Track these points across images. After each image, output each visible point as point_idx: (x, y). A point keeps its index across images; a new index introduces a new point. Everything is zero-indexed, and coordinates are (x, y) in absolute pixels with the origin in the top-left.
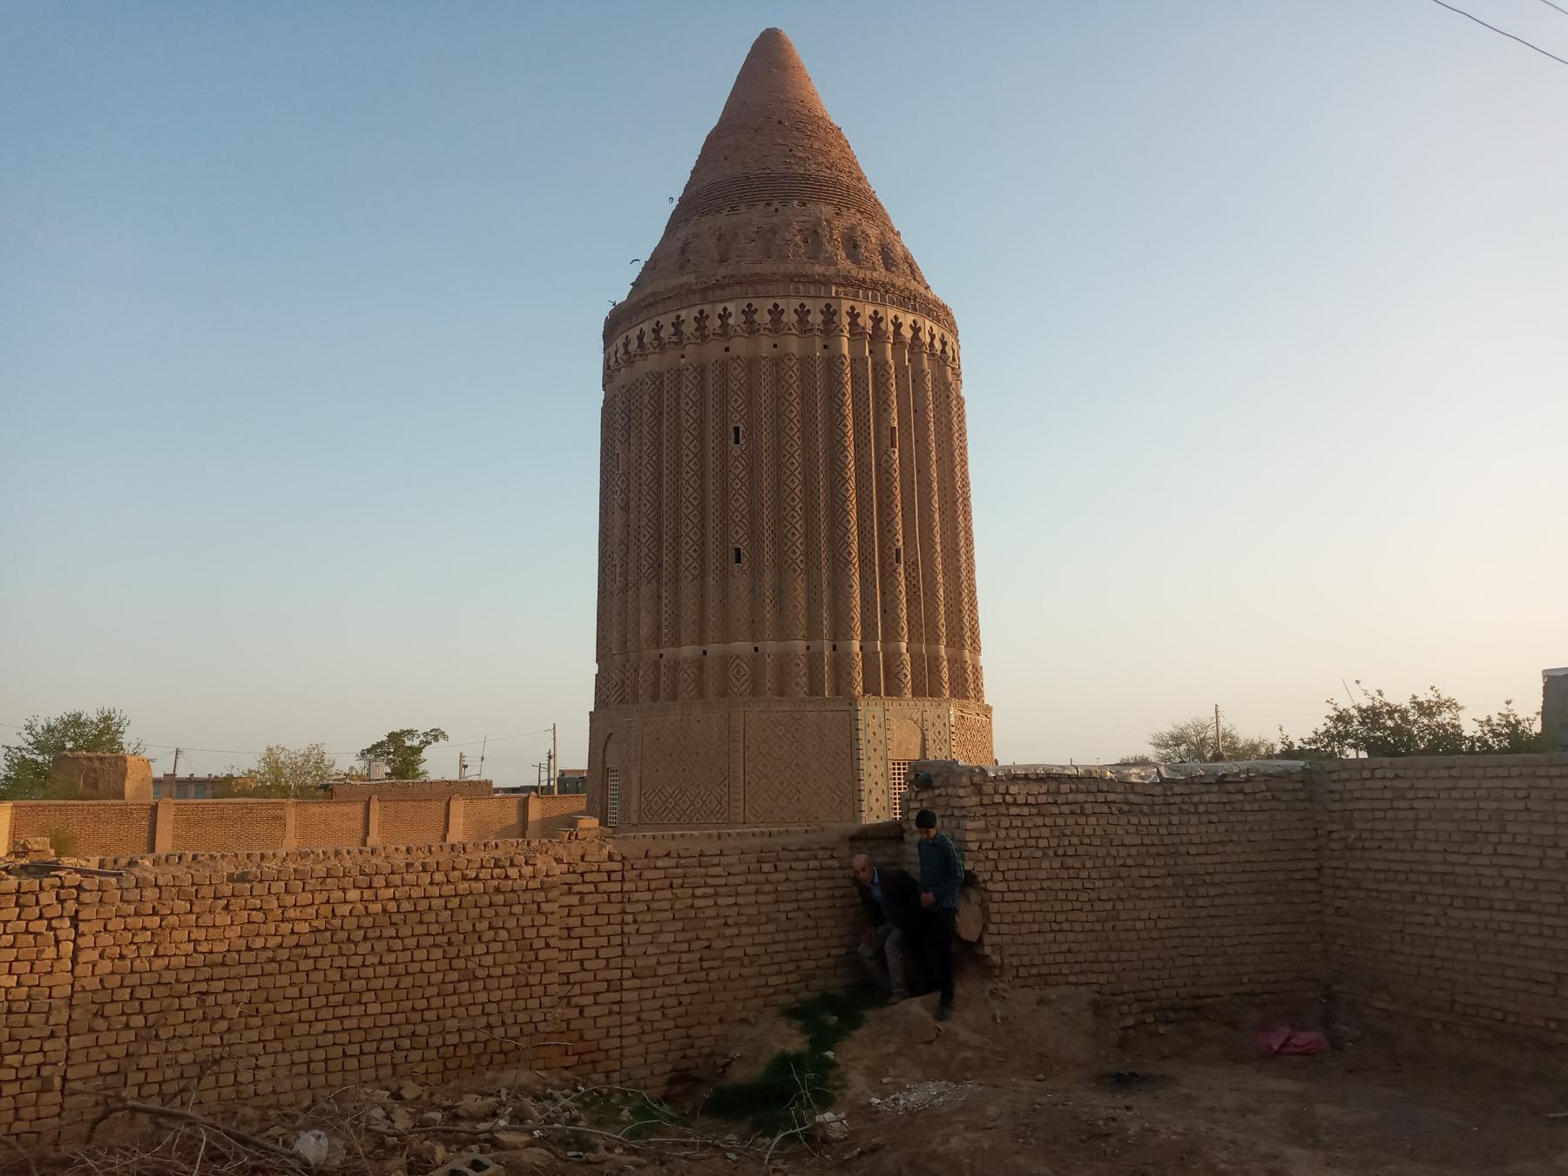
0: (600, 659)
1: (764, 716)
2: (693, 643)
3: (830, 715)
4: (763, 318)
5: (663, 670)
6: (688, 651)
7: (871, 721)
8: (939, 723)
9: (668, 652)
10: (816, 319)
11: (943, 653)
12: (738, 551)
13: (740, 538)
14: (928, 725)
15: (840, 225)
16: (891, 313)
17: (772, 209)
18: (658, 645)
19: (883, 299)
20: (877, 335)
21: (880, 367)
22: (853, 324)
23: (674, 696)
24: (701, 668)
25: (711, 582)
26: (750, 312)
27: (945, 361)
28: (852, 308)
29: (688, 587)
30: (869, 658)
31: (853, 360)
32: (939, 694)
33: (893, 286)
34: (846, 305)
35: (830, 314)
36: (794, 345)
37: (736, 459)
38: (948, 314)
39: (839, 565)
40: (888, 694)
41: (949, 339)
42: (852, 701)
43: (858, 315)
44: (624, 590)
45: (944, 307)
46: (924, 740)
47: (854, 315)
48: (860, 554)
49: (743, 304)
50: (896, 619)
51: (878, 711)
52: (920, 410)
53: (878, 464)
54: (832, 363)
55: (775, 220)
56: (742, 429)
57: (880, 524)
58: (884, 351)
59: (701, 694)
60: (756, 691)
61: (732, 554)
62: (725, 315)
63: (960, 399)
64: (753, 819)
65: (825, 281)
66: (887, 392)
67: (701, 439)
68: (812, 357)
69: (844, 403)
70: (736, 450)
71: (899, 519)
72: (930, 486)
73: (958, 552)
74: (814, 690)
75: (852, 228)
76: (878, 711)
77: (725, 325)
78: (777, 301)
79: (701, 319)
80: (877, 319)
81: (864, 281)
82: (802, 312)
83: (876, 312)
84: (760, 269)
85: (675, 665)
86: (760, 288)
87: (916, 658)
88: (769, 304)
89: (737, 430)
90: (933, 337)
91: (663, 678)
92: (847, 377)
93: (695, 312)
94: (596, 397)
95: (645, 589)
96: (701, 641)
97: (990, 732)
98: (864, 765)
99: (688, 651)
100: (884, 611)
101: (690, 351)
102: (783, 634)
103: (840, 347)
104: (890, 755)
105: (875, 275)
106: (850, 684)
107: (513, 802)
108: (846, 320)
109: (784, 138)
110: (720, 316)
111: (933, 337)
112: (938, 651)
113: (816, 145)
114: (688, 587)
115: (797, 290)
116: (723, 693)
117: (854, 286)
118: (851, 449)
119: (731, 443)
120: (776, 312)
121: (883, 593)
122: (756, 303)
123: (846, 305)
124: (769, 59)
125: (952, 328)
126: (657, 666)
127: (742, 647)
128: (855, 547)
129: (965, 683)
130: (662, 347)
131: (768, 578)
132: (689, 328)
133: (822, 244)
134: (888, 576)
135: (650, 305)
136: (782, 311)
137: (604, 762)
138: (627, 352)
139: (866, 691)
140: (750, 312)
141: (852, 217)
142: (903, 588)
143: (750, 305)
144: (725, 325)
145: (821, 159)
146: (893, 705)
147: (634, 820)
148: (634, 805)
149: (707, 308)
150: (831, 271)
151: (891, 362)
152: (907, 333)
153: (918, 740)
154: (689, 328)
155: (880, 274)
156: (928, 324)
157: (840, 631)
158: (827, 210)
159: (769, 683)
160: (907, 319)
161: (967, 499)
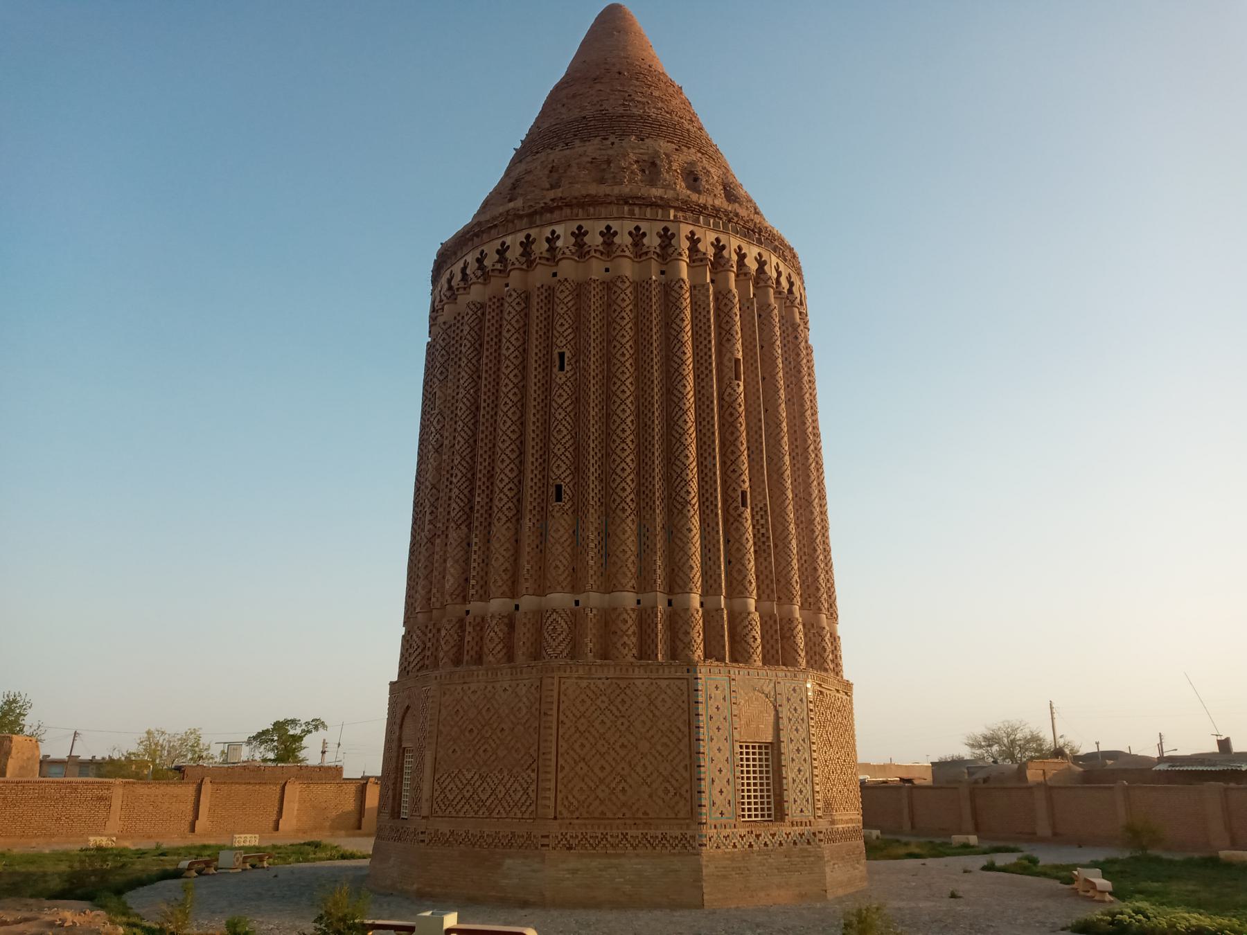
0: (406, 622)
1: (584, 683)
2: (503, 595)
3: (664, 684)
4: (594, 239)
5: (469, 629)
6: (497, 605)
7: (714, 692)
8: (795, 698)
9: (475, 606)
10: (652, 241)
11: (797, 614)
12: (559, 488)
13: (561, 472)
14: (782, 700)
15: (679, 161)
16: (733, 242)
17: (609, 142)
18: (465, 600)
20: (719, 263)
21: (722, 297)
22: (694, 249)
23: (479, 660)
24: (511, 626)
25: (527, 523)
26: (580, 234)
27: (791, 300)
28: (692, 233)
29: (501, 530)
30: (711, 616)
31: (693, 287)
32: (794, 663)
33: (737, 215)
34: (685, 229)
35: (667, 237)
36: (627, 268)
37: (561, 387)
38: (794, 256)
39: (675, 506)
40: (734, 660)
41: (794, 278)
42: (691, 667)
43: (699, 240)
44: (431, 541)
45: (791, 250)
46: (777, 718)
47: (694, 241)
48: (701, 496)
49: (573, 226)
50: (742, 572)
51: (722, 679)
52: (767, 346)
53: (721, 398)
54: (670, 289)
55: (610, 152)
56: (567, 354)
57: (723, 463)
58: (727, 280)
59: (510, 658)
60: (574, 652)
61: (552, 490)
62: (552, 239)
63: (808, 347)
64: (565, 813)
65: (663, 205)
66: (730, 323)
67: (523, 368)
68: (648, 281)
69: (682, 330)
70: (560, 377)
71: (744, 457)
72: (779, 425)
73: (810, 503)
74: (645, 652)
75: (692, 164)
76: (722, 679)
77: (552, 249)
78: (611, 223)
79: (527, 244)
80: (719, 247)
81: (705, 207)
82: (638, 235)
83: (718, 240)
84: (593, 189)
85: (481, 623)
86: (591, 210)
87: (767, 619)
88: (601, 226)
89: (562, 355)
90: (779, 274)
91: (468, 638)
92: (686, 302)
93: (521, 237)
94: (421, 337)
95: (453, 535)
96: (513, 593)
97: (851, 712)
98: (704, 747)
99: (497, 605)
100: (728, 562)
101: (515, 278)
102: (609, 585)
103: (679, 271)
104: (737, 736)
105: (717, 202)
106: (688, 645)
107: (352, 788)
108: (685, 244)
109: (621, 85)
110: (548, 240)
111: (779, 274)
112: (791, 612)
113: (656, 93)
114: (501, 530)
115: (632, 213)
116: (536, 654)
117: (697, 212)
118: (690, 378)
119: (556, 370)
120: (608, 234)
121: (727, 541)
122: (587, 225)
123: (685, 229)
124: (610, 28)
125: (799, 273)
126: (461, 623)
127: (560, 599)
128: (694, 485)
129: (823, 654)
130: (485, 275)
131: (593, 519)
132: (514, 253)
133: (659, 173)
134: (733, 521)
135: (477, 235)
136: (616, 233)
137: (400, 740)
138: (450, 288)
139: (707, 656)
140: (580, 234)
141: (691, 155)
142: (750, 535)
143: (580, 228)
144: (552, 249)
145: (660, 105)
146: (739, 673)
147: (425, 812)
148: (426, 793)
149: (533, 232)
150: (670, 194)
151: (735, 291)
152: (753, 266)
153: (771, 719)
154: (514, 253)
155: (720, 202)
156: (774, 260)
157: (676, 583)
158: (664, 146)
159: (590, 643)
160: (752, 251)
161: (817, 450)
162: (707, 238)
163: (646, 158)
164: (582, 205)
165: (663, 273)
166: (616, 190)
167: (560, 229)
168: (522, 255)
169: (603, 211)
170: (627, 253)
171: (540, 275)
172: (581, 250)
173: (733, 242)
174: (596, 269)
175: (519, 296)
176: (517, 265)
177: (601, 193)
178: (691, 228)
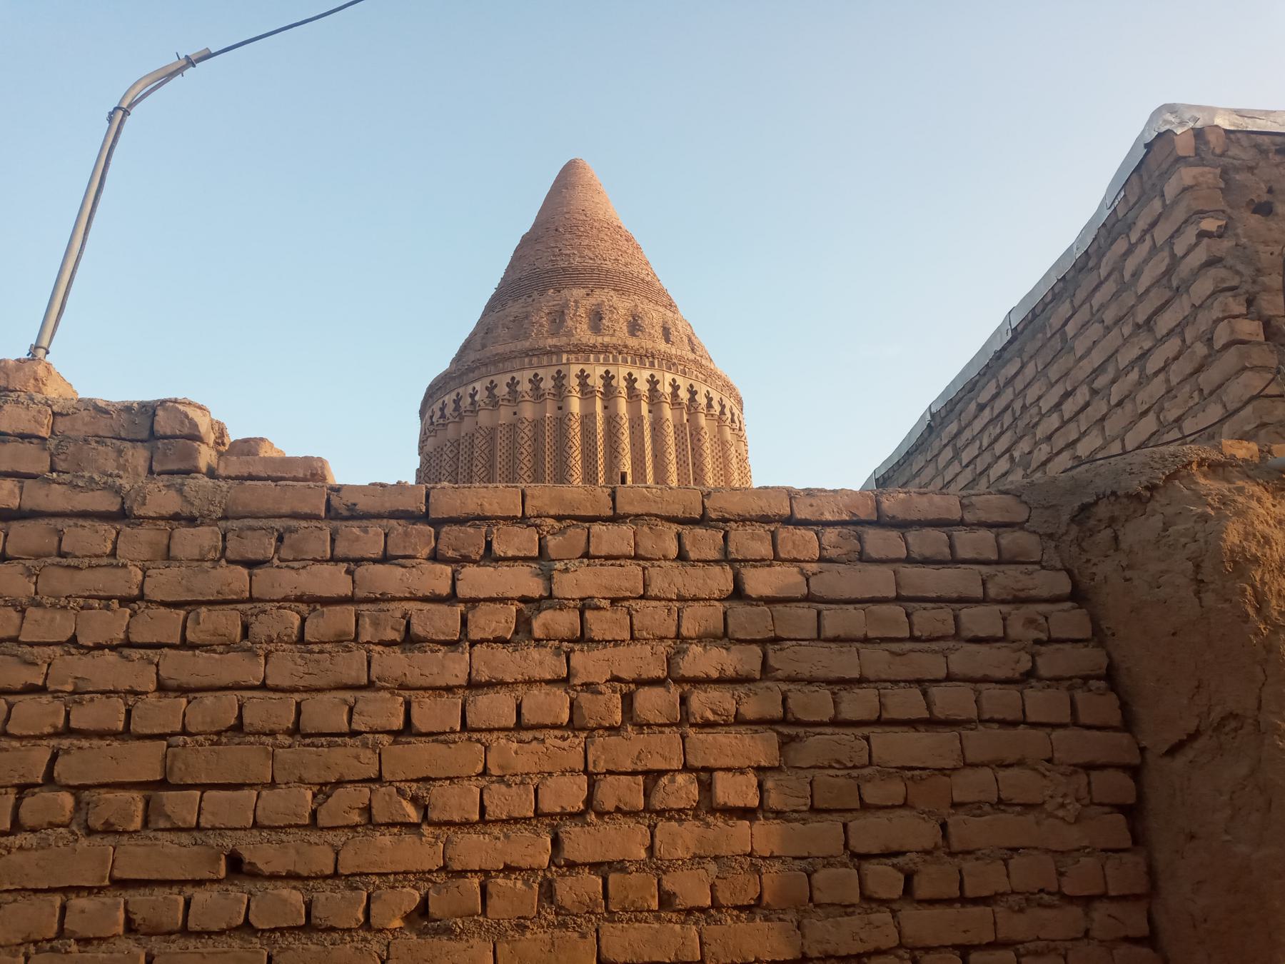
4: (502, 390)
10: (548, 384)
19: (615, 358)
21: (612, 421)
26: (491, 388)
33: (626, 346)
34: (575, 369)
35: (560, 378)
47: (583, 377)
49: (486, 382)
54: (562, 421)
55: (529, 309)
77: (473, 403)
82: (535, 381)
88: (507, 378)
93: (453, 395)
108: (574, 382)
117: (583, 351)
120: (513, 384)
122: (496, 379)
133: (564, 321)
141: (605, 296)
144: (473, 403)
149: (461, 390)
152: (642, 387)
158: (578, 293)
160: (642, 376)
162: (596, 373)
163: (557, 308)
164: (495, 363)
165: (560, 408)
166: (527, 344)
167: (478, 386)
168: (455, 410)
169: (508, 365)
170: (527, 398)
171: (467, 425)
172: (494, 402)
173: (621, 372)
174: (504, 415)
175: (452, 444)
176: (451, 419)
177: (508, 350)
178: (581, 366)
